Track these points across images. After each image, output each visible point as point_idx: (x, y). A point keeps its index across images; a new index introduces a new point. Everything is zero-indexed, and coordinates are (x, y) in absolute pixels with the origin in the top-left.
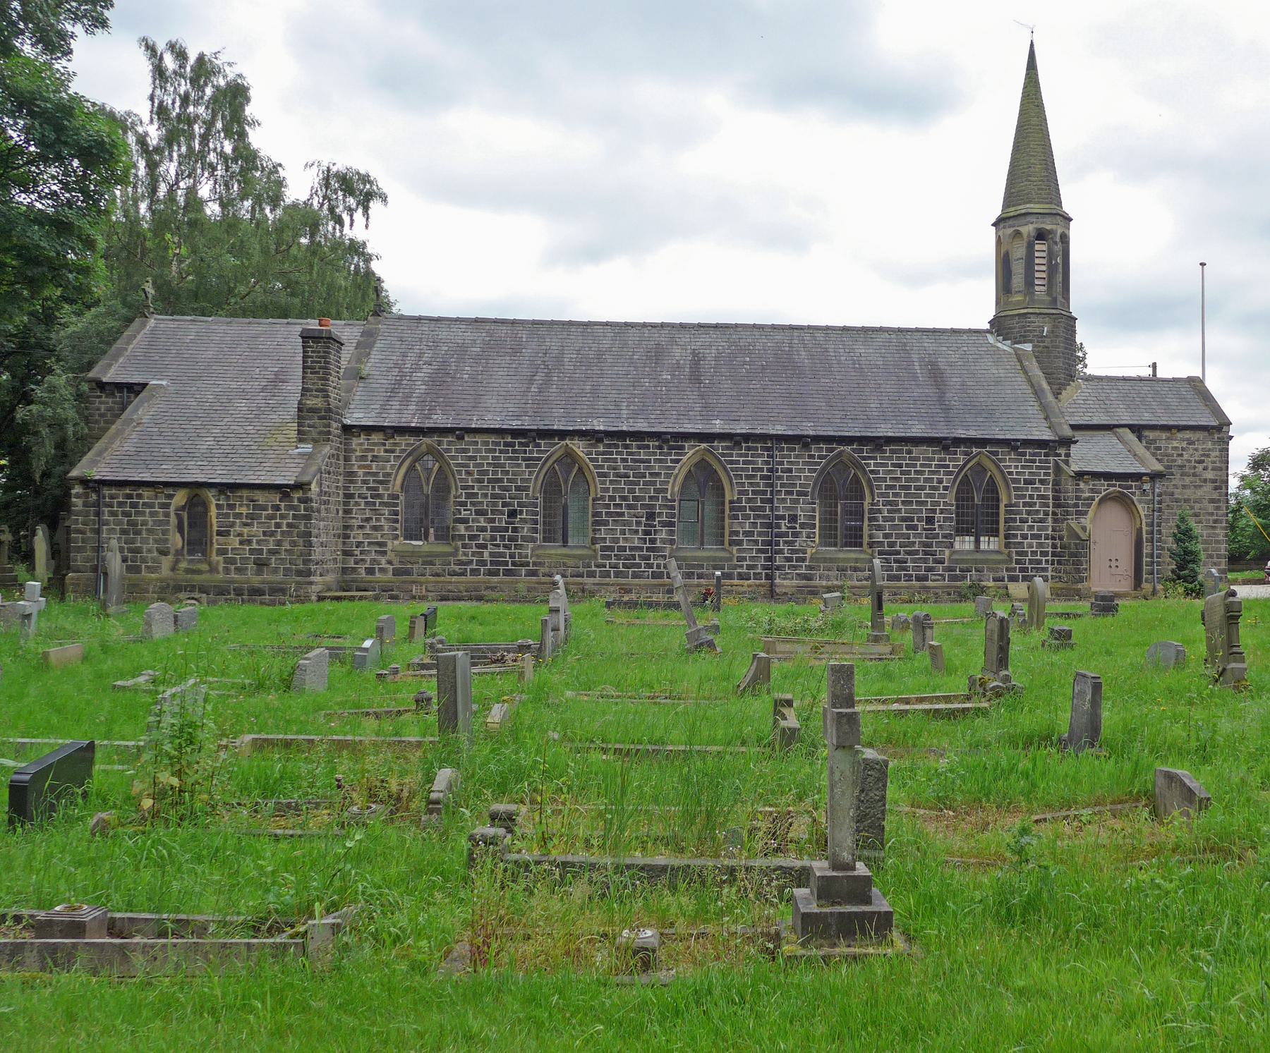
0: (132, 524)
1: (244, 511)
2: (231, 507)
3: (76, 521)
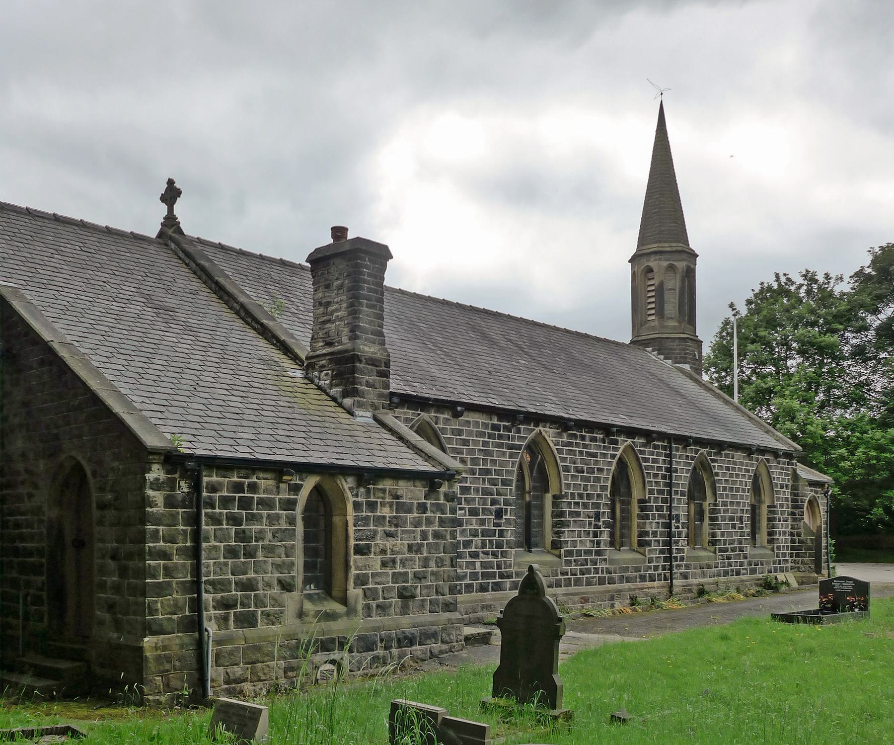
0: (242, 536)
1: (386, 512)
2: (372, 506)
3: (155, 536)
